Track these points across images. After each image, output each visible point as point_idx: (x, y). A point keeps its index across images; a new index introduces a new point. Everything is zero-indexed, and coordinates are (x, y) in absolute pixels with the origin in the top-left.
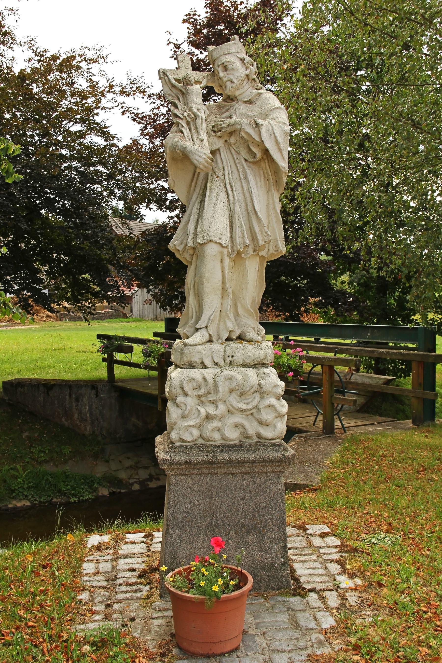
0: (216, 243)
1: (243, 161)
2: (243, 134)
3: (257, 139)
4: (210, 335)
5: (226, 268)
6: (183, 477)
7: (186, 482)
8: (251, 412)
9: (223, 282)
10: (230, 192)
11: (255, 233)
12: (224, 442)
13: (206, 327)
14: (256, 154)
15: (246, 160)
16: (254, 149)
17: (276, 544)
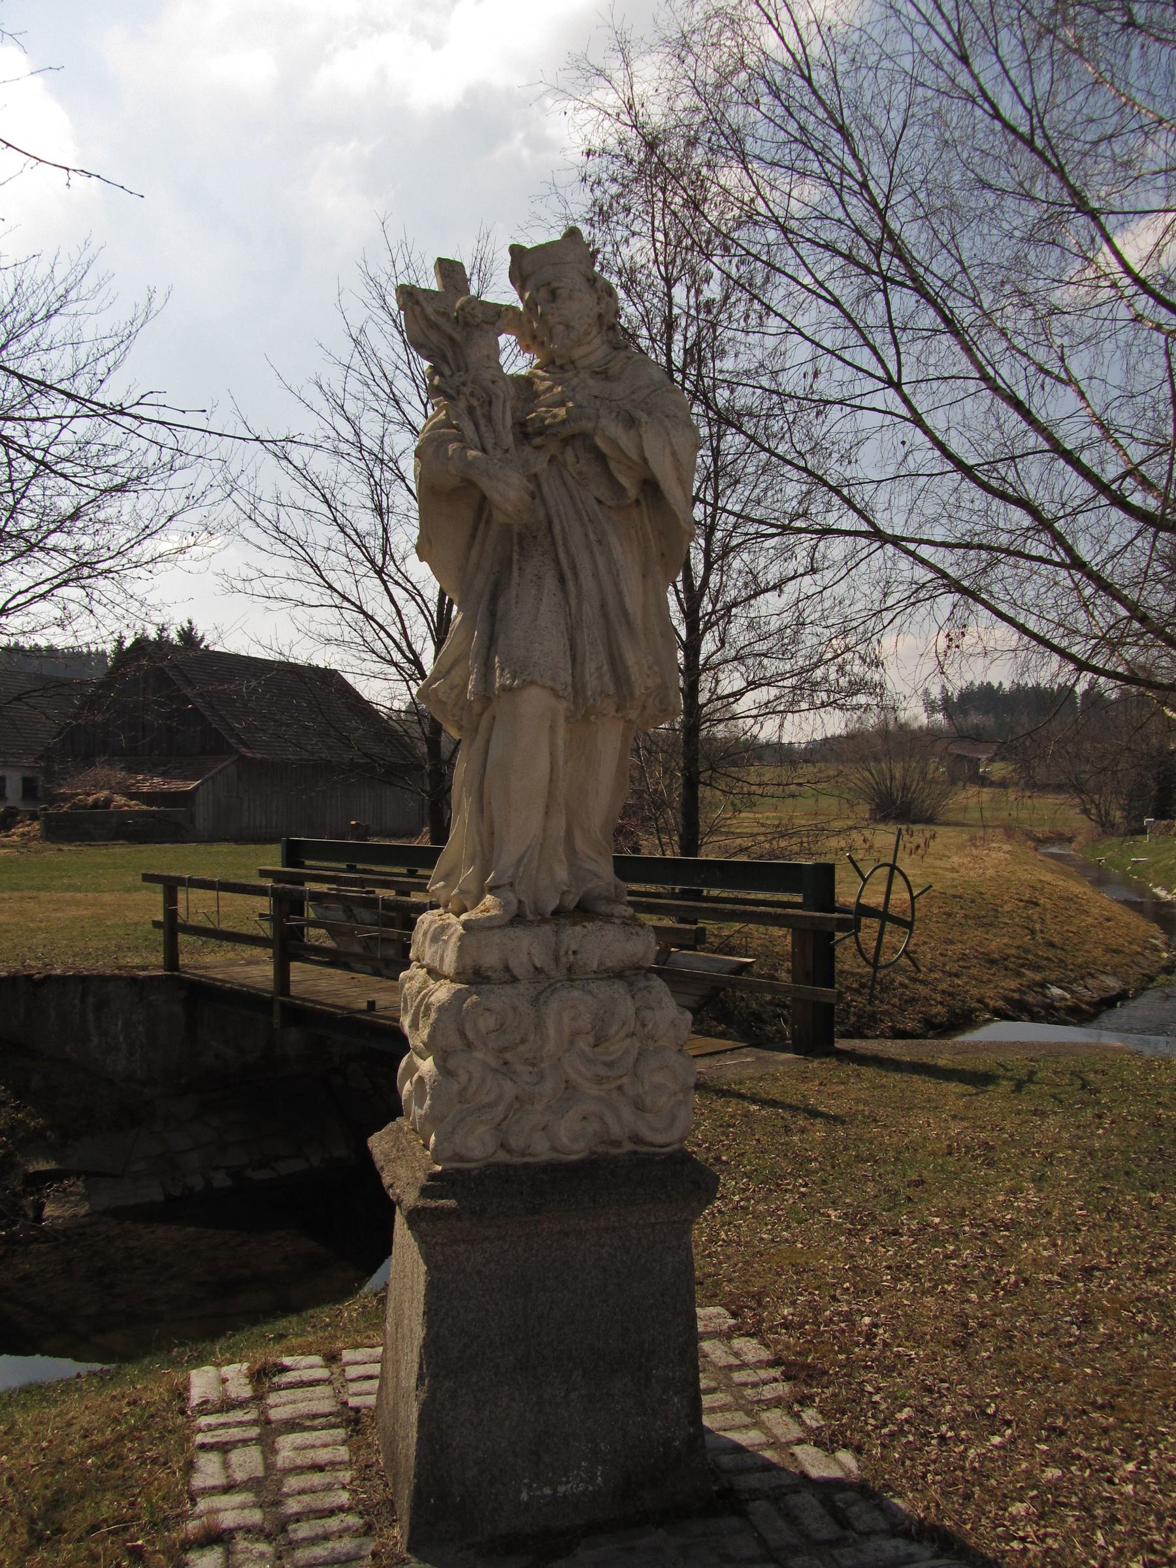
0: (543, 687)
1: (594, 502)
2: (599, 442)
3: (633, 454)
4: (520, 902)
5: (560, 743)
6: (461, 1248)
7: (468, 1259)
8: (618, 1083)
9: (551, 780)
10: (568, 574)
11: (626, 668)
12: (555, 1155)
13: (511, 884)
14: (623, 489)
15: (599, 502)
16: (624, 480)
17: (675, 1393)
